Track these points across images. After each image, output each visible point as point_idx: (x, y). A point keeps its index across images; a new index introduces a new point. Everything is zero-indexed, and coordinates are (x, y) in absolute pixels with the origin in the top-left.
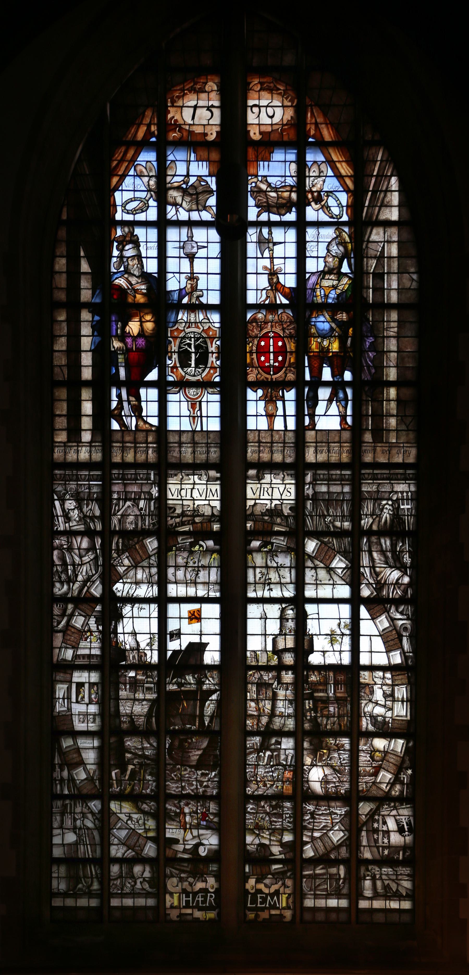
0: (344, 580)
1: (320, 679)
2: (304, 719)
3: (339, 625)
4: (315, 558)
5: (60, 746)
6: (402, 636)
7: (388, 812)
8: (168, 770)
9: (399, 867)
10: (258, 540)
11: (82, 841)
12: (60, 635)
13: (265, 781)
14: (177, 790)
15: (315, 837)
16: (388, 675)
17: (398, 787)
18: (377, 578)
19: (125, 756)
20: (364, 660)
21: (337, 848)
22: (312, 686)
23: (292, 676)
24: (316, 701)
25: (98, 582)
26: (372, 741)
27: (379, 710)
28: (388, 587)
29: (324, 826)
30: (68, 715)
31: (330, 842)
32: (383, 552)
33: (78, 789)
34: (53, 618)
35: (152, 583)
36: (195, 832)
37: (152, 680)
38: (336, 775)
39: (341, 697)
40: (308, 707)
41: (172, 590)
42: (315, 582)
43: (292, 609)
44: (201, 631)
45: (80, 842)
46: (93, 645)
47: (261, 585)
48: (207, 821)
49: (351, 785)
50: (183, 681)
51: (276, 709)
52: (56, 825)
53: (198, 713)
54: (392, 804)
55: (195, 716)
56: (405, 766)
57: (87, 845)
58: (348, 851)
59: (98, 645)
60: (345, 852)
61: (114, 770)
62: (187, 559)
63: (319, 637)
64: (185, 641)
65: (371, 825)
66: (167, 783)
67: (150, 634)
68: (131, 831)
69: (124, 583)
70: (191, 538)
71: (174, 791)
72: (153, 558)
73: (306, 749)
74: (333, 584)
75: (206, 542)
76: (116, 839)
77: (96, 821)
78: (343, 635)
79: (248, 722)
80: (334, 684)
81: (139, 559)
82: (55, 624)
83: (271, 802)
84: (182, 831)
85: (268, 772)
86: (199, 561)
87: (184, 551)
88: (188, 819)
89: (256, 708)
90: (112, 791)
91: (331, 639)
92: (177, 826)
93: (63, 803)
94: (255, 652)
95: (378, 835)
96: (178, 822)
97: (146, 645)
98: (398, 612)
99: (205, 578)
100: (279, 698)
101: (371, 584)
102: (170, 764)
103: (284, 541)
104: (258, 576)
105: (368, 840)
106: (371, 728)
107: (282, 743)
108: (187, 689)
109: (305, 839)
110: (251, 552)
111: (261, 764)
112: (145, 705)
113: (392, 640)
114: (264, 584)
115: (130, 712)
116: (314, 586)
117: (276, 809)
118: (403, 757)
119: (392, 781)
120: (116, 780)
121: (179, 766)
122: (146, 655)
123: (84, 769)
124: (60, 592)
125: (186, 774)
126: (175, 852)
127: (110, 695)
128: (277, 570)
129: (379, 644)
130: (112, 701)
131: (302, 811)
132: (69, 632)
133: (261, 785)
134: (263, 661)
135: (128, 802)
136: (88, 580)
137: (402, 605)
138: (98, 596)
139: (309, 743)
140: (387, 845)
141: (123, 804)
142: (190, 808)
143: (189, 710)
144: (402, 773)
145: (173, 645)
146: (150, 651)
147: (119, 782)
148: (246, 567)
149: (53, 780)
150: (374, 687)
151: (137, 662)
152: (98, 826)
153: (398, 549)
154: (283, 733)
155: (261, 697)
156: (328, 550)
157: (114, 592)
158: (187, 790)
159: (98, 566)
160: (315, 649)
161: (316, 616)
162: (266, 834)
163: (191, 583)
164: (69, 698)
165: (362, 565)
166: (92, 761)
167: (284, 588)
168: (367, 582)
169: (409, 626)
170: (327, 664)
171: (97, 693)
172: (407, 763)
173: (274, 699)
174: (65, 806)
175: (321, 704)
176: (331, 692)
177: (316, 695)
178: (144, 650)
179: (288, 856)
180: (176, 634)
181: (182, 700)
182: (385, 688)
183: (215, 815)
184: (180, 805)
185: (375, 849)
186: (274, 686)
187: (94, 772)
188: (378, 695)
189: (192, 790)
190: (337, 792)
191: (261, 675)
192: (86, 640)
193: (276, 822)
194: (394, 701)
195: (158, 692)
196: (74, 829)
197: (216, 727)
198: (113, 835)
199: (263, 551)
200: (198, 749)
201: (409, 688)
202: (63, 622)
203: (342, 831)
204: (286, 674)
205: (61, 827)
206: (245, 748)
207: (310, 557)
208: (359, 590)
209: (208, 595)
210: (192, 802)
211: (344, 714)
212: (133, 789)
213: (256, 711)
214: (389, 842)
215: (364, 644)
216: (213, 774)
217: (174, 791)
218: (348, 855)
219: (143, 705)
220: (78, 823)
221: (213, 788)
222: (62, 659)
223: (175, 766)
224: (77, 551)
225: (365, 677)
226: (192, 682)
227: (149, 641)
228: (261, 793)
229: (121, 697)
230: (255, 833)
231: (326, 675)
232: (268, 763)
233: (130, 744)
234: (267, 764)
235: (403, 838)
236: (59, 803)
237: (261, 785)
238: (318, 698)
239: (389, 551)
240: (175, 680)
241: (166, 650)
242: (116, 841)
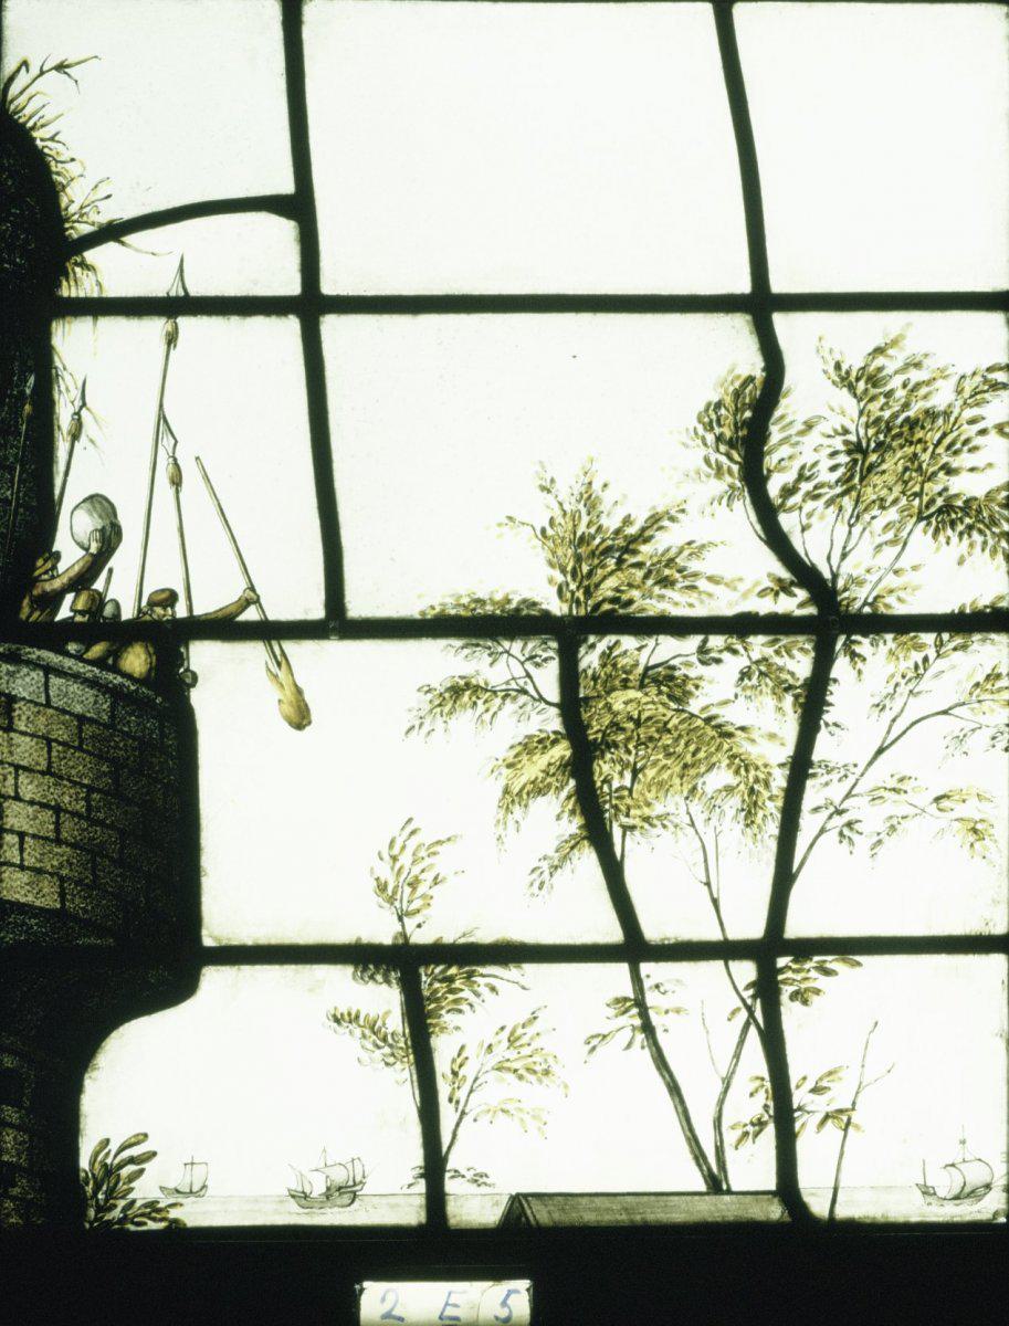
91: (571, 705)
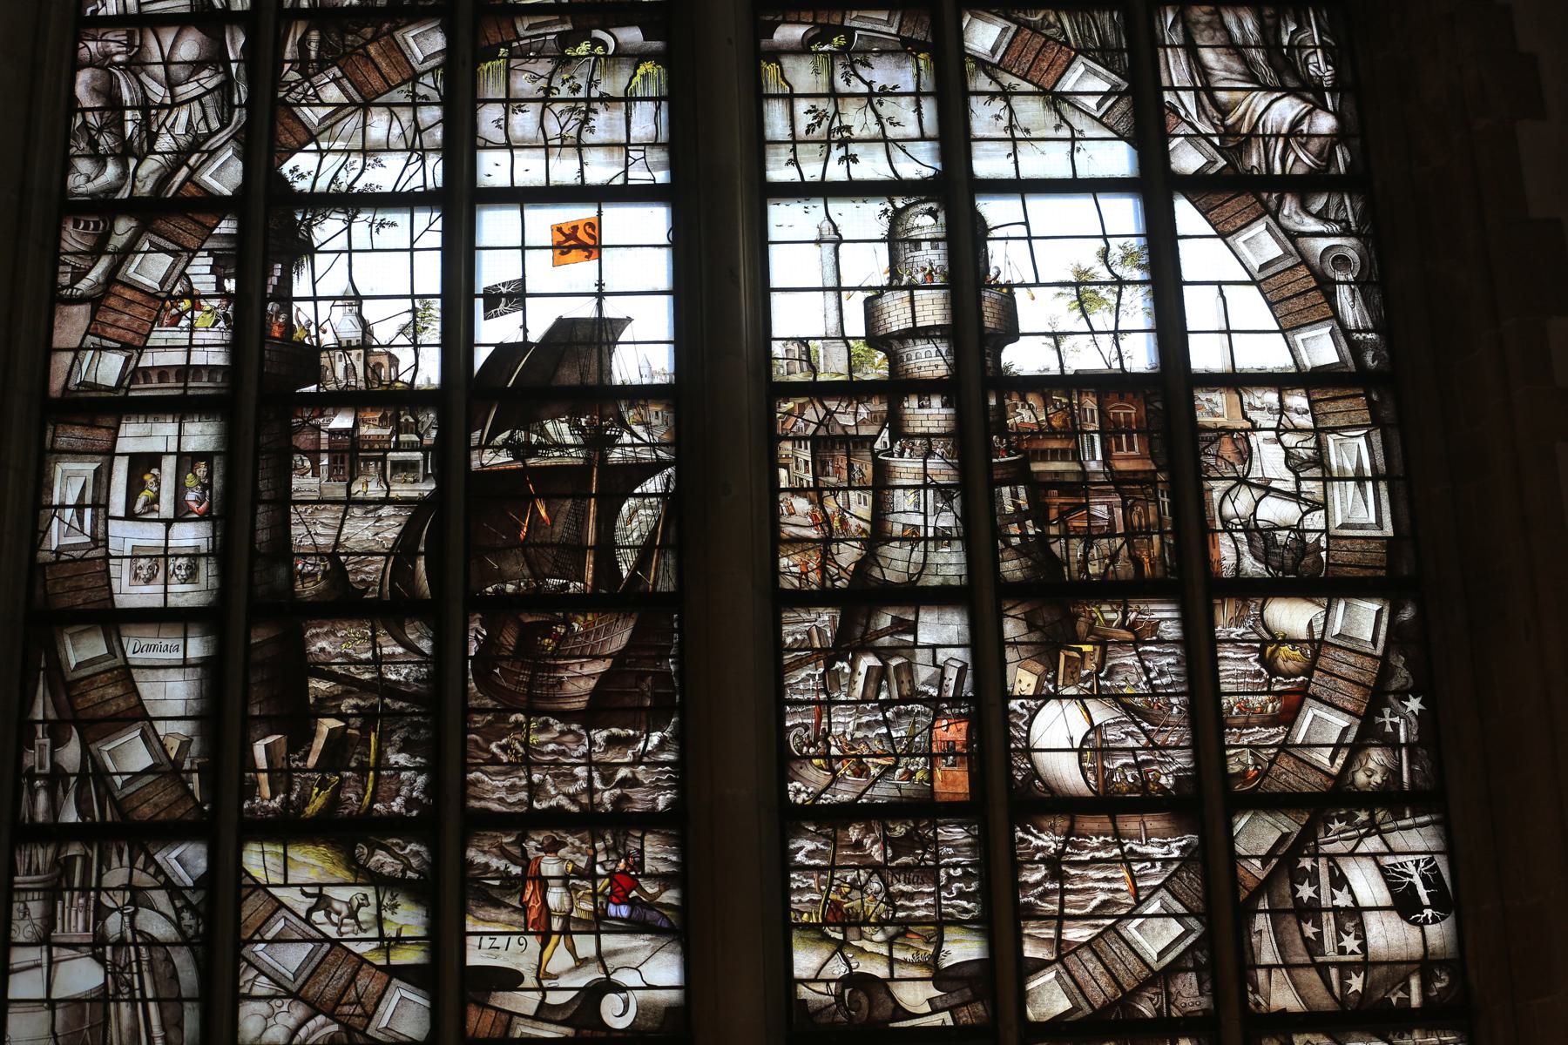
0: (1111, 129)
1: (1048, 419)
2: (1001, 545)
3: (1105, 255)
4: (1002, 66)
5: (56, 664)
6: (1336, 282)
7: (1350, 845)
8: (476, 731)
9: (1410, 1033)
10: (799, 22)
11: (125, 990)
12: (80, 313)
13: (859, 757)
14: (511, 799)
15: (1069, 943)
16: (1297, 400)
17: (1376, 758)
18: (1222, 121)
19: (307, 688)
20: (1205, 355)
21: (1161, 978)
22: (1020, 440)
23: (951, 411)
24: (1039, 487)
25: (230, 153)
26: (1262, 610)
27: (1275, 511)
28: (1266, 145)
29: (1104, 904)
30: (94, 559)
31: (1132, 958)
32: (1235, 49)
33: (117, 805)
34: (56, 262)
35: (422, 149)
36: (585, 945)
37: (415, 438)
38: (1138, 725)
39: (1135, 472)
40: (1010, 508)
41: (493, 169)
42: (1008, 135)
43: (931, 212)
44: (600, 284)
45: (117, 991)
46: (199, 337)
47: (817, 146)
48: (632, 903)
49: (1196, 757)
50: (534, 438)
51: (892, 517)
52: (23, 930)
53: (591, 538)
54: (1363, 816)
56: (1395, 685)
57: (145, 1001)
58: (1207, 986)
59: (219, 336)
60: (1194, 990)
61: (264, 737)
62: (550, 80)
63: (1033, 289)
64: (540, 319)
65: (1287, 890)
66: (471, 776)
67: (413, 297)
68: (327, 946)
69: (322, 153)
70: (564, 22)
71: (501, 800)
72: (429, 80)
73: (1015, 644)
74: (1073, 140)
75: (615, 31)
76: (263, 979)
77: (186, 915)
78: (1120, 283)
79: (784, 562)
80: (1101, 432)
81: (377, 82)
82: (65, 279)
83: (886, 828)
84: (533, 943)
85: (869, 725)
86: (591, 83)
87: (538, 57)
88: (555, 897)
89: (814, 517)
90: (251, 810)
91: (1078, 296)
92: (511, 924)
93: (58, 852)
94: (803, 342)
95: (1318, 924)
96: (516, 910)
97: (396, 331)
98: (1309, 214)
99: (612, 131)
100: (898, 482)
101: (1206, 137)
102: (483, 711)
103: (888, 23)
104: (803, 121)
105: (1282, 946)
106: (1251, 566)
107: (920, 627)
108: (548, 462)
109: (1030, 951)
110: (776, 55)
111: (843, 698)
112: (389, 517)
113: (1296, 295)
114: (828, 142)
115: (332, 541)
116: (1008, 147)
117: (910, 852)
118: (1384, 659)
119: (1350, 738)
120: (270, 771)
121: (521, 717)
122: (394, 361)
123: (144, 736)
124: (91, 187)
125: (546, 743)
126: (504, 1017)
127: (256, 492)
128: (870, 102)
129: (1251, 308)
130: (261, 509)
131: (1013, 854)
132: (113, 302)
133: (843, 768)
134: (833, 365)
135: (316, 844)
136: (196, 146)
137: (1320, 192)
138: (227, 192)
139: (1022, 624)
140: (1359, 958)
141: (295, 853)
142: (563, 860)
143: (558, 529)
144: (1387, 711)
145: (493, 331)
146: (411, 351)
147: (281, 776)
148: (759, 98)
149: (22, 778)
150: (1252, 439)
151: (362, 385)
152: (191, 932)
153: (1286, 40)
154: (916, 595)
155: (833, 480)
156: (1044, 45)
157: (283, 178)
158: (552, 797)
159: (232, 107)
160: (1023, 328)
161: (1022, 231)
162: (875, 941)
163: (562, 146)
164: (100, 504)
165: (1166, 83)
166: (178, 709)
167: (897, 154)
168: (1191, 131)
169: (1352, 255)
170: (1069, 371)
171: (206, 487)
172: (1402, 677)
173: (881, 485)
174: (63, 867)
175: (1060, 495)
176: (1094, 458)
177: (1037, 467)
178: (389, 346)
179: (965, 1016)
180: (509, 296)
181: (532, 498)
182: (1290, 439)
183: (665, 880)
184: (524, 851)
185: (1312, 976)
186: (878, 445)
187: (185, 745)
188: (1270, 460)
189: (573, 798)
190: (1143, 784)
191: (829, 413)
192: (175, 322)
193: (910, 896)
194: (1327, 478)
195: (441, 476)
196: (96, 946)
197: (662, 579)
198: (251, 965)
199: (817, 52)
200: (595, 658)
201: (1376, 438)
202: (97, 273)
203: (1178, 917)
204: (921, 407)
205: (45, 940)
206: (779, 647)
207: (982, 64)
208: (1165, 156)
209: (626, 179)
210: (570, 839)
211: (1148, 526)
212: (334, 801)
213: (814, 526)
214: (1363, 946)
215: (1199, 308)
216: (655, 738)
217: (501, 800)
218: (1205, 1002)
219: (379, 519)
220: (114, 924)
221: (656, 787)
222: (82, 383)
223: (502, 714)
224: (159, 71)
225: (1215, 408)
226: (569, 439)
227: (408, 318)
228: (846, 797)
229: (296, 496)
230: (827, 938)
231: (1070, 405)
232: (870, 694)
233: (329, 648)
234: (864, 700)
235: (1416, 931)
236: (42, 855)
237: (843, 768)
238: (1048, 479)
239: (1255, 47)
240: (507, 434)
241: (471, 345)
242: (263, 986)
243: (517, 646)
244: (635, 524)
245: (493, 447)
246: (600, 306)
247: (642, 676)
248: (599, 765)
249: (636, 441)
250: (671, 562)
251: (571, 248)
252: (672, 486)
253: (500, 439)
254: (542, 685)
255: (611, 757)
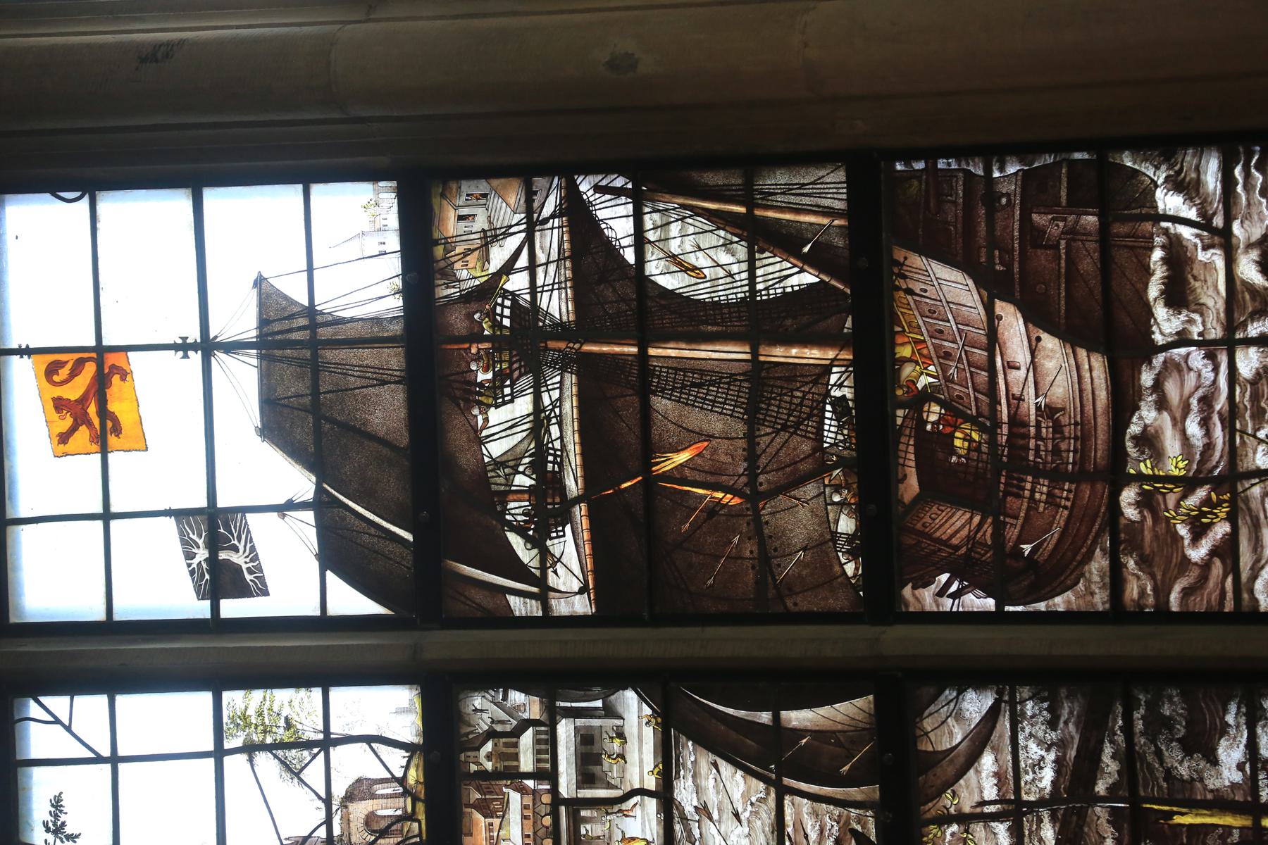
8: (1162, 592)
37: (527, 739)
44: (183, 347)
53: (735, 352)
55: (758, 373)
67: (219, 753)
97: (293, 787)
112: (698, 790)
121: (1128, 496)
122: (361, 790)
125: (1185, 439)
143: (716, 424)
146: (336, 753)
178: (328, 801)
180: (215, 543)
181: (651, 483)
216: (1169, 202)
219: (703, 810)
226: (523, 405)
240: (515, 540)
241: (324, 624)
243: (971, 504)
244: (701, 260)
245: (543, 569)
246: (232, 347)
247: (1033, 236)
248: (1231, 325)
249: (523, 261)
250: (781, 178)
251: (104, 413)
252: (619, 182)
253: (526, 555)
254: (1056, 451)
255: (1213, 296)
